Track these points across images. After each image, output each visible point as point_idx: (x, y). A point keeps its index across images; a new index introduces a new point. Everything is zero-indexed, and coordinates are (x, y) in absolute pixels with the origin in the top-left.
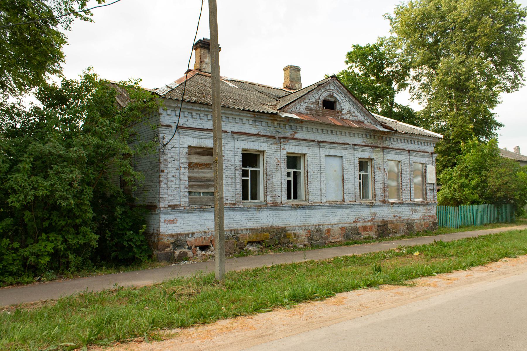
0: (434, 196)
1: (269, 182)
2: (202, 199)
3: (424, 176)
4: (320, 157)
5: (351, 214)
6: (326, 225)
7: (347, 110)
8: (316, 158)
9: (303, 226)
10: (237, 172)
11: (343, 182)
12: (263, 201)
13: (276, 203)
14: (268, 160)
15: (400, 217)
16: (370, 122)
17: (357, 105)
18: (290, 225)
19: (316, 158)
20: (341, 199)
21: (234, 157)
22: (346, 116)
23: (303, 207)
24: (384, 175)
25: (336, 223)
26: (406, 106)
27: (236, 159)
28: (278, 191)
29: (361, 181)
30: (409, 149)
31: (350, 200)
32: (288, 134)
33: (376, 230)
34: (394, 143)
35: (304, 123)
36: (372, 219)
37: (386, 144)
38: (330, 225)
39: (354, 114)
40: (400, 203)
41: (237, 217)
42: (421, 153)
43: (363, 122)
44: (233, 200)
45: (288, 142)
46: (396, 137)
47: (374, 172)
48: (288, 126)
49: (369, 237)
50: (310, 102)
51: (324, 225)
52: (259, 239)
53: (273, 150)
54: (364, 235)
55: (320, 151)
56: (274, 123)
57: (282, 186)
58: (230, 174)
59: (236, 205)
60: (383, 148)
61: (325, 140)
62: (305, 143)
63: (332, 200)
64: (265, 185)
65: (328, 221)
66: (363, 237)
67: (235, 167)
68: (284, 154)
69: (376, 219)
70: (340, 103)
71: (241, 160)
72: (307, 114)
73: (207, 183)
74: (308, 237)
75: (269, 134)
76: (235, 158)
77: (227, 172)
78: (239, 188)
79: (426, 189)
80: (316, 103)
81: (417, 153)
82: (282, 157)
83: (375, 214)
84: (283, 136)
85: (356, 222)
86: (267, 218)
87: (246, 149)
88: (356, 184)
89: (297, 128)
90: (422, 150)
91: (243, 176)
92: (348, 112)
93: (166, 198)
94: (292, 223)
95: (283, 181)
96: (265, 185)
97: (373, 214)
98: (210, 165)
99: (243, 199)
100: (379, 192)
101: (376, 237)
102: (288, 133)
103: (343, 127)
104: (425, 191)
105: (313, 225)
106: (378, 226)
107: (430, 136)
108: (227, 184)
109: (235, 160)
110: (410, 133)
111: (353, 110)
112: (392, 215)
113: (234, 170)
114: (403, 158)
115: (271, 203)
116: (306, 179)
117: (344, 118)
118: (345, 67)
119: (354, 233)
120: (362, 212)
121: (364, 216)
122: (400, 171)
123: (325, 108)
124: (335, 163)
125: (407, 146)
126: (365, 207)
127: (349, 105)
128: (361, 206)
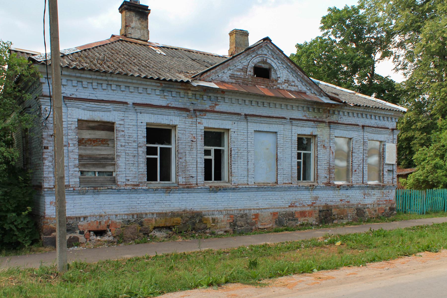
0: (393, 178)
1: (181, 160)
2: (96, 179)
3: (382, 156)
4: (248, 133)
5: (286, 198)
6: (254, 209)
7: (284, 78)
8: (243, 134)
9: (224, 210)
10: (140, 149)
11: (277, 161)
12: (175, 182)
13: (190, 185)
14: (180, 136)
15: (348, 202)
16: (314, 93)
17: (297, 73)
18: (208, 210)
19: (243, 134)
20: (275, 181)
21: (136, 132)
22: (283, 86)
23: (225, 189)
24: (330, 154)
25: (266, 207)
26: (386, 77)
27: (139, 135)
28: (193, 171)
29: (302, 161)
30: (364, 124)
31: (285, 182)
32: (206, 106)
33: (317, 215)
34: (344, 118)
35: (226, 93)
36: (313, 203)
37: (334, 118)
38: (259, 209)
39: (293, 84)
40: (348, 185)
41: (140, 200)
42: (379, 129)
43: (305, 93)
44: (136, 181)
45: (205, 115)
46: (347, 111)
47: (317, 151)
48: (206, 97)
49: (307, 224)
50: (236, 69)
51: (251, 210)
53: (187, 125)
54: (301, 220)
55: (248, 126)
56: (188, 93)
57: (198, 166)
58: (131, 152)
59: (139, 186)
60: (330, 123)
61: (254, 113)
62: (227, 116)
63: (263, 182)
64: (177, 165)
65: (257, 205)
66: (299, 223)
67: (138, 144)
68: (202, 130)
69: (318, 203)
70: (275, 71)
71: (146, 135)
72: (232, 83)
73: (103, 162)
74: (230, 223)
75: (182, 106)
76: (137, 133)
77: (128, 149)
78: (143, 168)
79: (383, 170)
80: (244, 70)
81: (373, 129)
82: (198, 133)
83: (316, 198)
84: (200, 108)
85: (293, 206)
86: (179, 201)
87: (151, 123)
88: (293, 164)
89: (218, 99)
90: (380, 126)
91: (147, 154)
92: (285, 80)
93: (51, 177)
94: (210, 207)
95: (199, 160)
96: (177, 165)
97: (315, 198)
98: (107, 141)
99: (148, 180)
100: (323, 173)
101: (317, 223)
102: (207, 105)
103: (277, 98)
104: (382, 173)
105: (238, 210)
106: (320, 211)
107: (390, 110)
108: (128, 162)
109: (138, 136)
110: (363, 106)
111: (291, 78)
112: (338, 199)
113: (137, 147)
114: (355, 134)
115: (183, 185)
116: (230, 158)
117: (281, 88)
118: (320, 34)
119: (289, 219)
120: (300, 196)
121: (303, 200)
122: (351, 149)
123: (255, 76)
124: (268, 140)
125: (361, 121)
126: (304, 190)
127: (287, 72)
128: (298, 188)
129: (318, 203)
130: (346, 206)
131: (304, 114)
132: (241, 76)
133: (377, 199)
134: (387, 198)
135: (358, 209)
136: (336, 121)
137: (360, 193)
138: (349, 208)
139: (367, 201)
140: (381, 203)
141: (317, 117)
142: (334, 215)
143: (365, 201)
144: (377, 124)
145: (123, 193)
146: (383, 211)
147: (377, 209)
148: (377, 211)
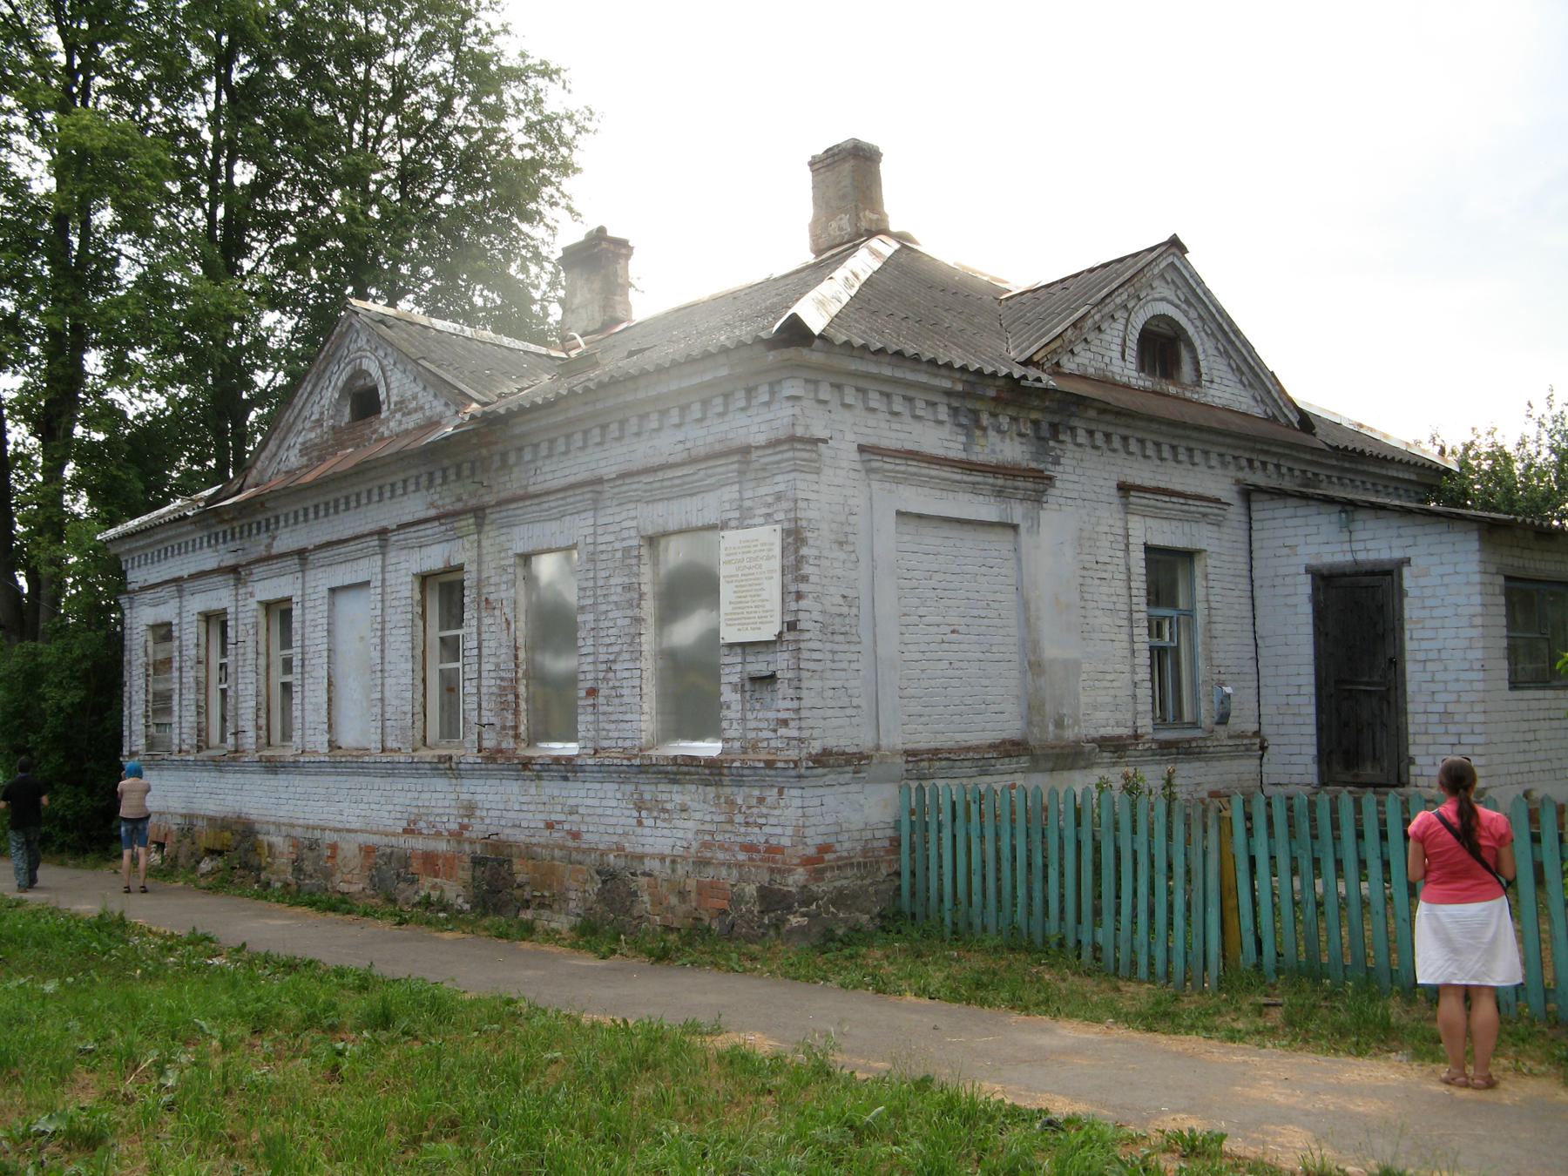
15: (576, 836)
22: (392, 424)
33: (465, 875)
52: (218, 847)
54: (426, 885)
63: (354, 745)
69: (477, 830)
90: (702, 451)
97: (466, 808)
106: (477, 862)
119: (398, 875)
129: (476, 827)
131: (429, 499)
132: (317, 441)
133: (698, 832)
134: (756, 836)
135: (609, 876)
136: (521, 492)
138: (571, 863)
139: (651, 840)
140: (721, 856)
141: (465, 497)
142: (519, 886)
144: (688, 445)
145: (177, 769)
146: (725, 904)
147: (691, 884)
148: (693, 895)
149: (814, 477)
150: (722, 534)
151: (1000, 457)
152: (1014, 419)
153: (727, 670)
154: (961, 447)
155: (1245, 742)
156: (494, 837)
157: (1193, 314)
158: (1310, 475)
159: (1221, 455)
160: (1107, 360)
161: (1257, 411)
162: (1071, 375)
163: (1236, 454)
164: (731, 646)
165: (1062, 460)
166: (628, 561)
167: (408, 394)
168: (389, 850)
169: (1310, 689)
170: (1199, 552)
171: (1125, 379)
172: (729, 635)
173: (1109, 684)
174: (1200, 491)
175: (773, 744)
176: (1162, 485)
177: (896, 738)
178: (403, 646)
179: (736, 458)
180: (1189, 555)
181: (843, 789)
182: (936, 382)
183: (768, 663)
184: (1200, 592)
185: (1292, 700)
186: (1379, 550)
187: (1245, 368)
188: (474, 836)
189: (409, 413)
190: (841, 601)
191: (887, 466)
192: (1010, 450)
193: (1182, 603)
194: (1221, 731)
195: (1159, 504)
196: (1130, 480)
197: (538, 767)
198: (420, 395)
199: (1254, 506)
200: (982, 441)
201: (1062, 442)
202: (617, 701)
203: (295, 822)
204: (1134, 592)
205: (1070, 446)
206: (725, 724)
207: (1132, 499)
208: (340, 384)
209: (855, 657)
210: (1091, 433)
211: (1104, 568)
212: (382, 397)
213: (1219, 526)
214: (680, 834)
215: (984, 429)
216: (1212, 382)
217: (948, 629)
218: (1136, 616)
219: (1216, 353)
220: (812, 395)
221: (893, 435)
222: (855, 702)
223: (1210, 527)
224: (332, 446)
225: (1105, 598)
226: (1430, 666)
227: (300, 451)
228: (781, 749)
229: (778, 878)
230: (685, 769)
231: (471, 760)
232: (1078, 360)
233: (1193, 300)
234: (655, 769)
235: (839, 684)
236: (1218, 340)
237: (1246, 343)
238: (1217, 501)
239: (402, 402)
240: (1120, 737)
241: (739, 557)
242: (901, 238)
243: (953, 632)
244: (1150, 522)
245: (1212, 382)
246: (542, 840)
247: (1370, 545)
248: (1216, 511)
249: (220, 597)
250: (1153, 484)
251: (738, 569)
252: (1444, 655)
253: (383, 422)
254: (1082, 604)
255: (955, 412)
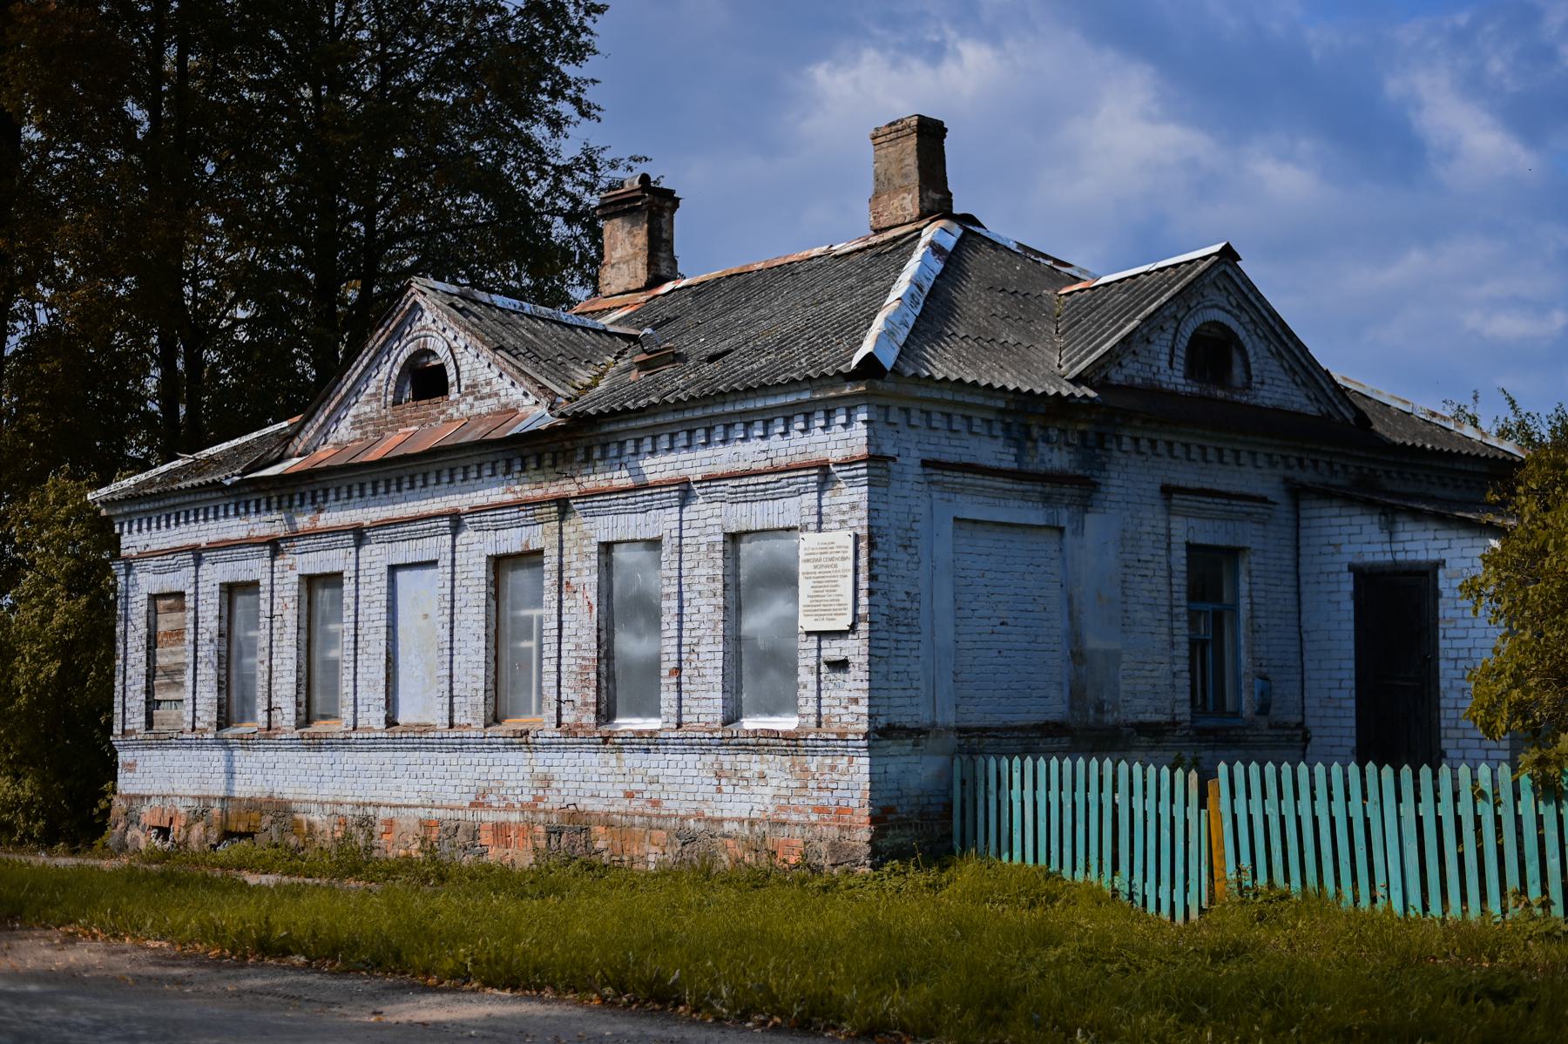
15: (656, 803)
22: (462, 407)
69: (553, 801)
83: (547, 781)
120: (500, 769)
130: (641, 820)
132: (372, 415)
134: (826, 799)
137: (699, 765)
140: (795, 818)
142: (597, 853)
143: (720, 806)
144: (771, 455)
149: (884, 490)
150: (801, 535)
151: (1049, 466)
152: (1063, 431)
153: (804, 655)
154: (1013, 458)
155: (1287, 732)
156: (572, 808)
157: (1245, 318)
158: (1365, 471)
159: (1269, 456)
160: (1155, 369)
161: (1311, 409)
162: (1119, 387)
163: (1285, 453)
164: (809, 633)
165: (1107, 466)
166: (713, 555)
167: (481, 379)
168: (454, 824)
169: (1350, 684)
170: (1244, 549)
171: (1172, 387)
172: (807, 623)
173: (1148, 674)
174: (1245, 490)
175: (844, 719)
176: (1206, 486)
177: (948, 717)
178: (476, 624)
179: (816, 471)
180: (1233, 554)
181: (904, 759)
182: (991, 403)
183: (841, 649)
184: (1244, 587)
185: (1334, 693)
186: (1417, 551)
187: (1297, 368)
188: (549, 807)
189: (482, 398)
190: (904, 597)
191: (946, 479)
192: (1058, 459)
193: (1226, 596)
194: (1263, 722)
195: (1202, 505)
196: (1174, 483)
197: (620, 741)
198: (494, 381)
199: (1303, 504)
200: (1032, 453)
201: (1108, 450)
202: (699, 680)
203: (342, 800)
204: (1175, 588)
205: (1116, 454)
206: (801, 702)
207: (1174, 501)
208: (401, 360)
209: (915, 645)
210: (1136, 440)
211: (1144, 565)
212: (452, 378)
213: (1264, 524)
214: (758, 799)
215: (1035, 441)
216: (1262, 383)
217: (998, 622)
218: (1176, 610)
219: (1268, 354)
220: (883, 418)
221: (952, 450)
222: (915, 684)
223: (1255, 526)
224: (392, 422)
225: (1147, 594)
226: (1461, 664)
227: (352, 424)
228: (852, 724)
229: (846, 834)
230: (763, 741)
231: (549, 734)
232: (1125, 371)
233: (1245, 305)
234: (735, 741)
235: (901, 668)
236: (1271, 342)
237: (1300, 345)
238: (1263, 500)
239: (474, 386)
240: (1158, 724)
241: (818, 556)
242: (967, 220)
243: (1002, 624)
244: (1193, 522)
245: (1262, 383)
246: (622, 809)
247: (1408, 546)
248: (1261, 510)
249: (253, 567)
250: (1198, 485)
251: (815, 567)
252: (1474, 654)
253: (452, 404)
254: (1124, 599)
255: (1007, 428)
